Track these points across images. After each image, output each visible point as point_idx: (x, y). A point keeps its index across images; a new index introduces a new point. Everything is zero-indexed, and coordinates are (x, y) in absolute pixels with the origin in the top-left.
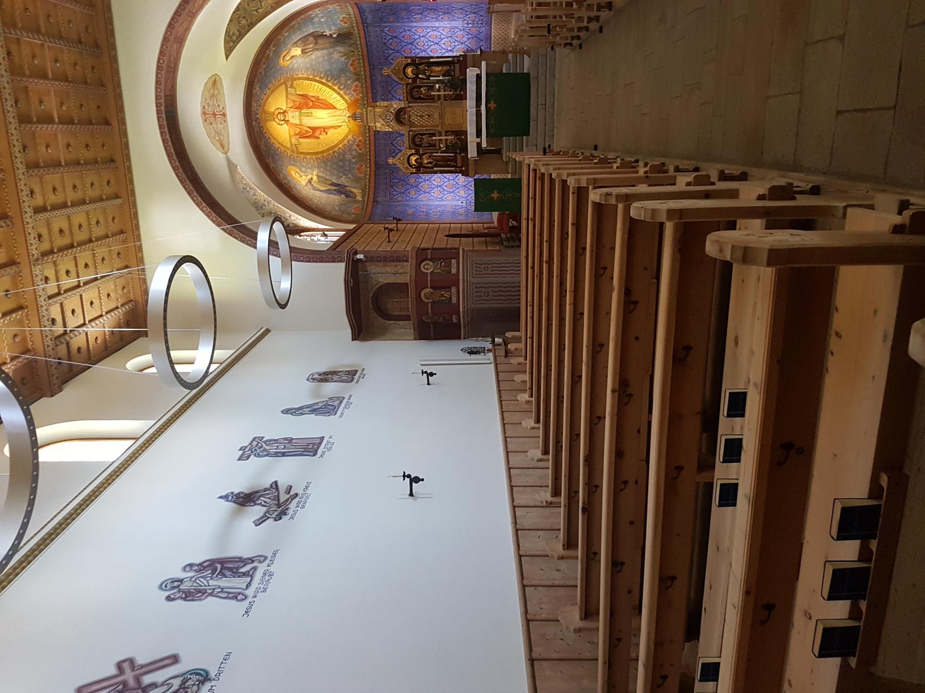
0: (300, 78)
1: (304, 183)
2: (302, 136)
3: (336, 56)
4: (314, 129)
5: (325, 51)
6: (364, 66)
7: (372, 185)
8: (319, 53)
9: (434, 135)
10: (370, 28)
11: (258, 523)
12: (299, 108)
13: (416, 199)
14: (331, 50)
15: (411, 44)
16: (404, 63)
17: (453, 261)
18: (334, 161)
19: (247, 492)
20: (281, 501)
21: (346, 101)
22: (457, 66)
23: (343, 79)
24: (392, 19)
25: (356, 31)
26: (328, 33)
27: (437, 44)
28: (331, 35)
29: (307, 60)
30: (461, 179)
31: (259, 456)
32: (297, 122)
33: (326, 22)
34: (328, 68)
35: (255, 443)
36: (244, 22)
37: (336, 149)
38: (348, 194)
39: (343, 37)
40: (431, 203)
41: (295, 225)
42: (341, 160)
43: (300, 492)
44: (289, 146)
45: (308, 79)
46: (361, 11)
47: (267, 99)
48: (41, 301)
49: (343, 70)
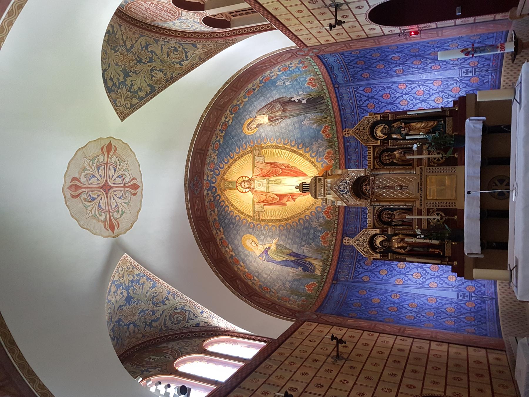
0: (269, 147)
2: (267, 203)
3: (307, 123)
4: (281, 196)
5: (295, 119)
6: (337, 133)
7: (336, 258)
8: (289, 121)
9: (409, 211)
10: (343, 90)
12: (267, 175)
13: (387, 282)
14: (302, 117)
15: (391, 104)
16: (372, 120)
18: (299, 228)
21: (317, 168)
22: (450, 121)
23: (315, 147)
24: (366, 75)
25: (327, 95)
26: (296, 99)
27: (424, 101)
28: (300, 101)
29: (276, 128)
30: (452, 278)
32: (263, 189)
33: (293, 86)
34: (299, 136)
36: (160, 75)
37: (303, 216)
38: (307, 267)
39: (313, 102)
40: (406, 290)
41: (207, 325)
42: (306, 228)
44: (251, 214)
45: (278, 147)
46: (329, 69)
47: (229, 167)
49: (315, 138)
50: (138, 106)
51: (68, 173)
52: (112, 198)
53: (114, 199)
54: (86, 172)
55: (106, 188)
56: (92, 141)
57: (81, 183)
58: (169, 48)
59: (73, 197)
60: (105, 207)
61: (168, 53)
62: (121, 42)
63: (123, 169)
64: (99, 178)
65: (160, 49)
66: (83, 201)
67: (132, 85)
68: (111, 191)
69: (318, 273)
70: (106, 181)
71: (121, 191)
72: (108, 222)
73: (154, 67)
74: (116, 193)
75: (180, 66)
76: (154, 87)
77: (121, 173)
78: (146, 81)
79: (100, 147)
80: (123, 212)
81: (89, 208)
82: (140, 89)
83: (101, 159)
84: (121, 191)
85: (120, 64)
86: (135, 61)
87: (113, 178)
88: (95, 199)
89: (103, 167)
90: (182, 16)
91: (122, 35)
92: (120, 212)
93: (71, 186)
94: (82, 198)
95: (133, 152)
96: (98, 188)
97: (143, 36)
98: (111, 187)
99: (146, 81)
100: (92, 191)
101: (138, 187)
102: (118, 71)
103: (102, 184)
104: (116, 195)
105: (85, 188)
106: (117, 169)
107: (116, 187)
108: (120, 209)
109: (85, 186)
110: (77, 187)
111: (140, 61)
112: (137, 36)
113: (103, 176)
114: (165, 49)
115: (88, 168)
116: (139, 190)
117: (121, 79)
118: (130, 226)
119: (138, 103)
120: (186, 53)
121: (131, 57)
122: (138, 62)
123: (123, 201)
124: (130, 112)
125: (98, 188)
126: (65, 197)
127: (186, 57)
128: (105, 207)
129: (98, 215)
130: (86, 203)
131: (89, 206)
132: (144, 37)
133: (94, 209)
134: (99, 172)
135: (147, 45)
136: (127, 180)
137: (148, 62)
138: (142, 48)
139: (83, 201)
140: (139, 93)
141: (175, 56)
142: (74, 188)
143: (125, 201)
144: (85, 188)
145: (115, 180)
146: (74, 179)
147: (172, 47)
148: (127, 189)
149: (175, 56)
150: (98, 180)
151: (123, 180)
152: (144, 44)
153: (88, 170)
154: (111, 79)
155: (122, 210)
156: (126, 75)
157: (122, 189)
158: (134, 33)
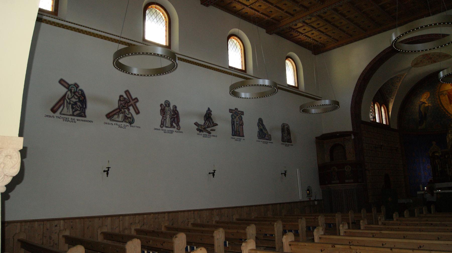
1: (422, 100)
11: (196, 124)
17: (352, 181)
19: (212, 117)
20: (207, 129)
31: (232, 116)
35: (239, 113)
43: (211, 134)
48: (301, 20)
69: (420, 128)
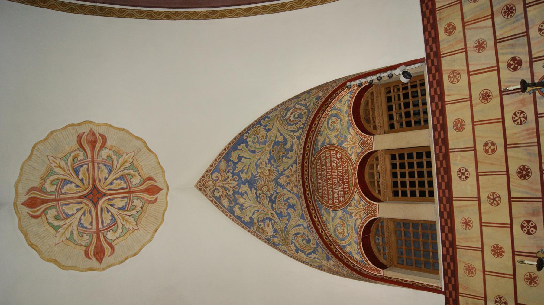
36: (270, 231)
50: (221, 208)
51: (111, 129)
52: (79, 206)
53: (78, 210)
54: (115, 157)
55: (94, 195)
56: (157, 159)
57: (99, 151)
58: (304, 234)
59: (78, 136)
60: (66, 193)
61: (299, 233)
62: (281, 168)
63: (124, 223)
64: (109, 181)
65: (297, 224)
66: (74, 154)
67: (242, 194)
68: (90, 204)
70: (105, 195)
71: (91, 223)
72: (41, 196)
73: (274, 221)
74: (87, 214)
75: (294, 250)
76: (252, 226)
77: (119, 221)
78: (253, 214)
79: (152, 175)
80: (56, 228)
81: (63, 164)
82: (241, 208)
83: (136, 180)
84: (91, 223)
85: (259, 171)
86: (269, 195)
87: (110, 208)
88: (77, 175)
89: (125, 186)
90: (350, 205)
91: (288, 168)
92: (56, 223)
93: (94, 134)
94: (77, 152)
95: (153, 236)
96: (94, 181)
97: (298, 199)
98: (95, 204)
99: (253, 214)
100: (88, 170)
101: (100, 260)
102: (252, 170)
103: (99, 187)
104: (84, 214)
105: (93, 157)
106: (125, 213)
107: (97, 215)
108: (62, 223)
109: (95, 157)
110: (93, 143)
111: (272, 201)
112: (295, 190)
113: (112, 187)
114: (301, 230)
115: (121, 160)
116: (94, 262)
117: (244, 176)
118: (33, 241)
119: (224, 207)
120: (313, 252)
121: (271, 187)
122: (270, 198)
123: (75, 228)
124: (211, 197)
125: (94, 181)
126: (79, 124)
127: (309, 254)
128: (66, 193)
129: (52, 178)
130: (70, 159)
131: (67, 164)
132: (298, 201)
133: (62, 172)
134: (116, 179)
135: (291, 206)
136: (110, 235)
137: (276, 212)
138: (286, 201)
139: (74, 154)
140: (237, 207)
141: (301, 242)
142: (92, 140)
143: (75, 232)
144: (93, 157)
145: (108, 211)
146: (104, 139)
147: (308, 236)
148: (95, 236)
149: (301, 242)
150: (106, 179)
151: (109, 227)
152: (292, 202)
153: (118, 160)
154: (240, 158)
155: (60, 227)
156: (251, 183)
157: (94, 227)
158: (296, 186)
